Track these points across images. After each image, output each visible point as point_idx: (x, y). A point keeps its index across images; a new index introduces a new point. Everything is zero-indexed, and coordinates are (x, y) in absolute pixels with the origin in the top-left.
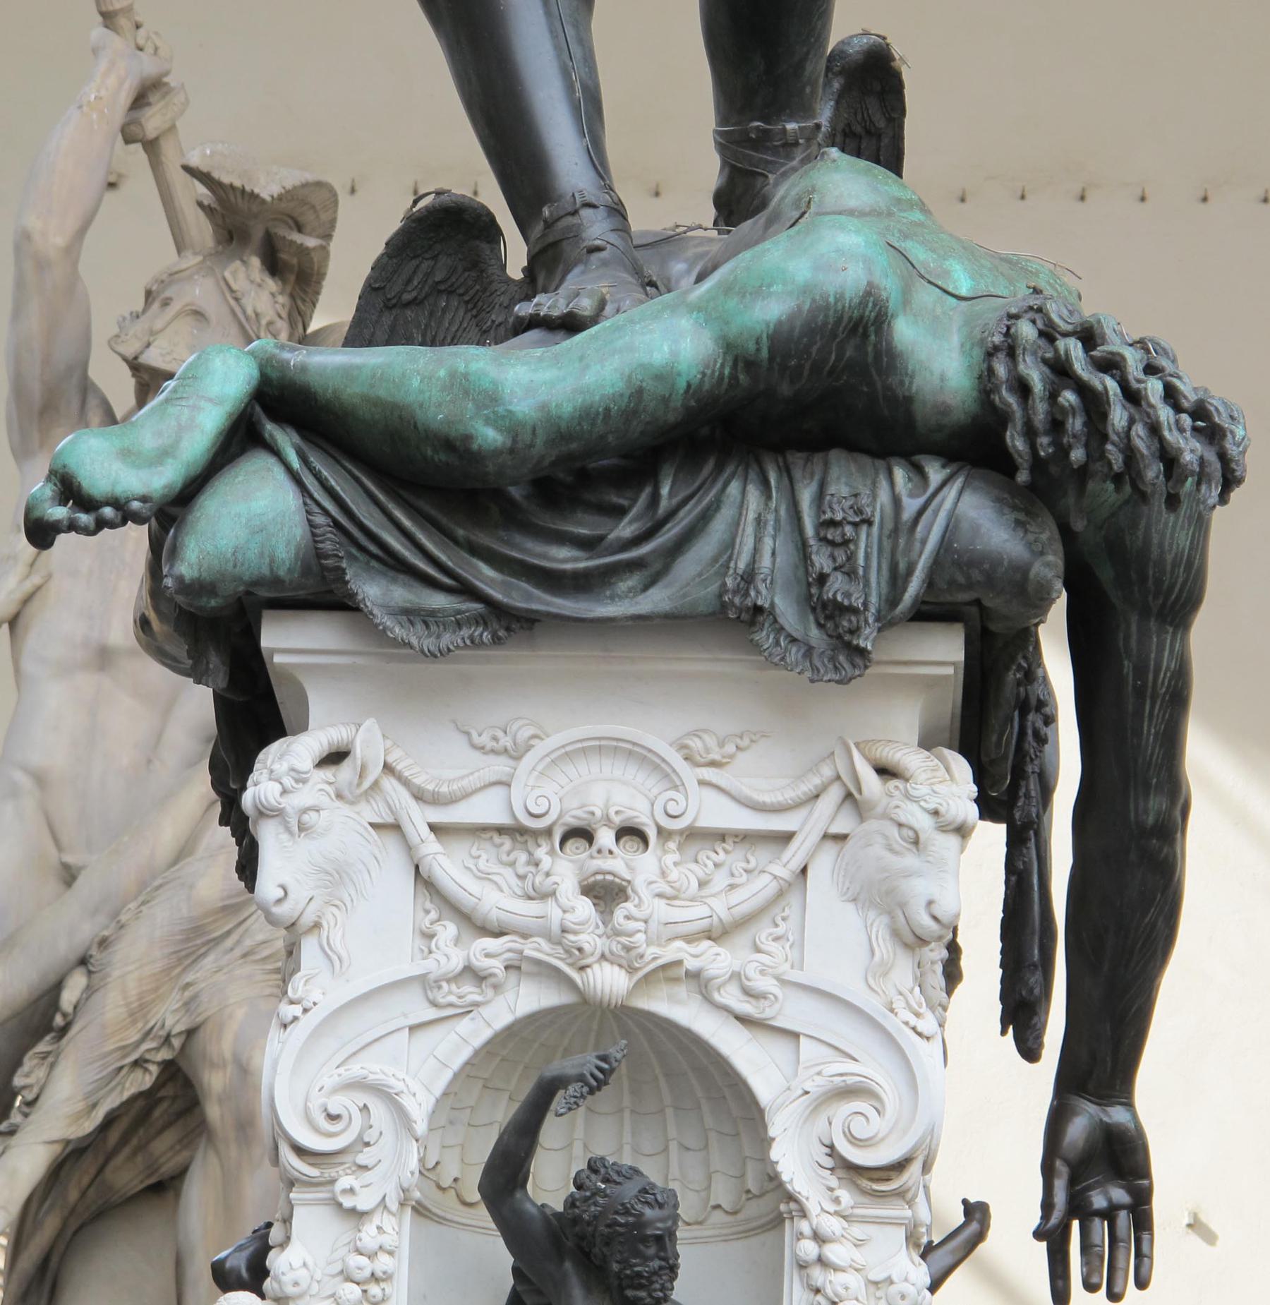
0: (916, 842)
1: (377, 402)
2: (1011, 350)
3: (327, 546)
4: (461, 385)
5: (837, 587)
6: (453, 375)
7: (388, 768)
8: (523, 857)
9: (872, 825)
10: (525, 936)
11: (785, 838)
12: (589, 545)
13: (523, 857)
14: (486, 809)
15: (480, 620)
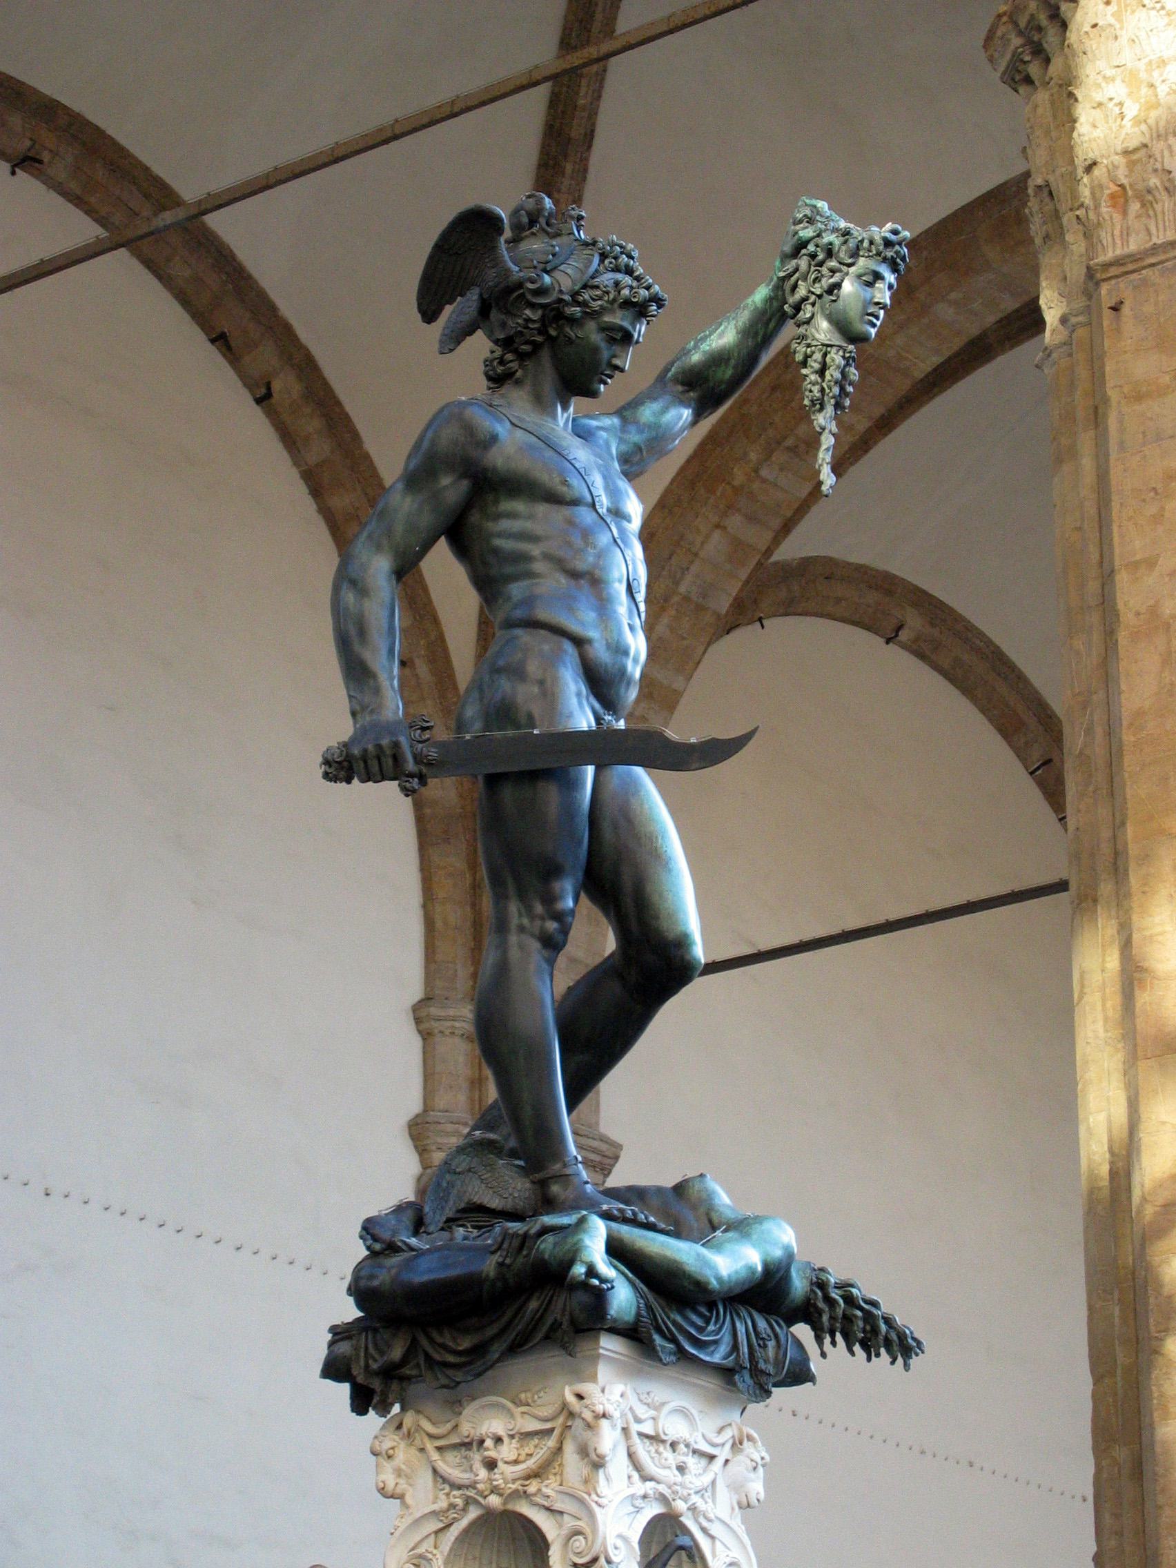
0: (755, 1468)
1: (665, 1257)
2: (822, 1285)
3: (644, 1313)
4: (707, 1263)
5: (762, 1365)
6: (698, 1255)
7: (631, 1409)
8: (653, 1449)
9: (740, 1457)
10: (658, 1482)
11: (712, 1458)
12: (701, 1330)
13: (653, 1449)
14: (648, 1428)
15: (675, 1354)
